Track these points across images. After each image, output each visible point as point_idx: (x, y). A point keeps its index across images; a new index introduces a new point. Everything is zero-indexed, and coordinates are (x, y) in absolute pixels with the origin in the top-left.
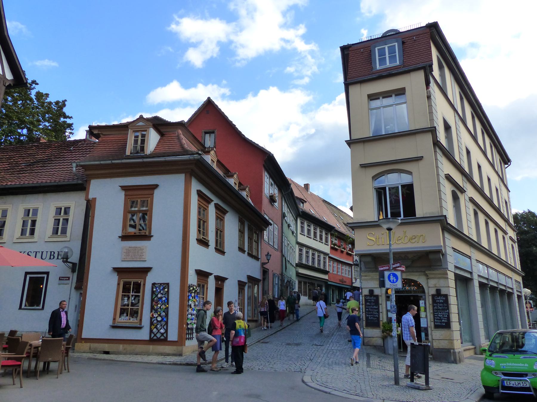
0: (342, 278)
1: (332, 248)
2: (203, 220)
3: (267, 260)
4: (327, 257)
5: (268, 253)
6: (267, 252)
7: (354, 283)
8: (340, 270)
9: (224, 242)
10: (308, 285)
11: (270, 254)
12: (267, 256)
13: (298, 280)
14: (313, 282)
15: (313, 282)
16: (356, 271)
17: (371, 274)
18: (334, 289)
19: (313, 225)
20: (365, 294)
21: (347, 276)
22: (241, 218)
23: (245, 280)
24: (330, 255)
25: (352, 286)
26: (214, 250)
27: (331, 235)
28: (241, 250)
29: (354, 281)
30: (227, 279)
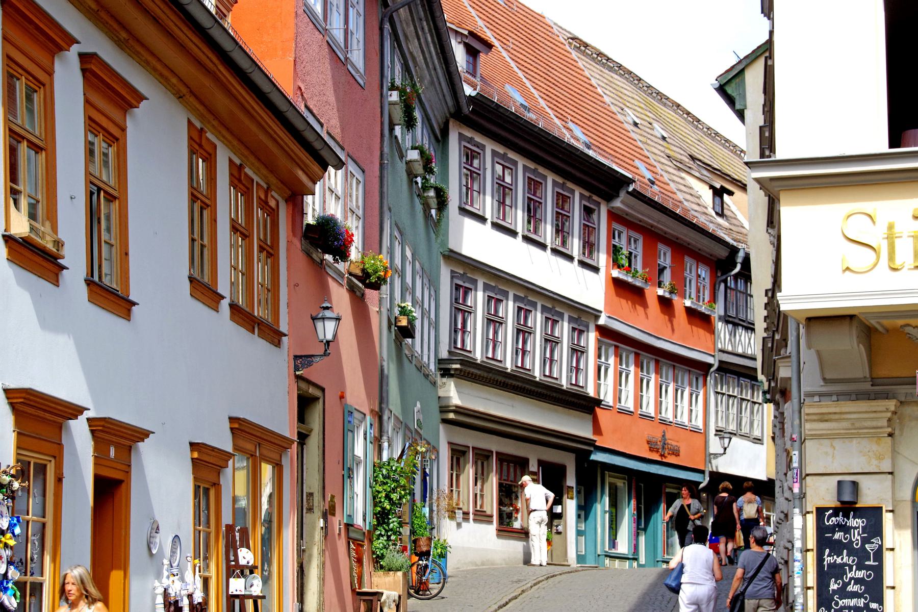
2: (28, 141)
7: (716, 456)
8: (650, 395)
13: (449, 443)
18: (620, 483)
22: (201, 131)
26: (83, 289)
27: (614, 216)
29: (715, 445)
30: (143, 435)
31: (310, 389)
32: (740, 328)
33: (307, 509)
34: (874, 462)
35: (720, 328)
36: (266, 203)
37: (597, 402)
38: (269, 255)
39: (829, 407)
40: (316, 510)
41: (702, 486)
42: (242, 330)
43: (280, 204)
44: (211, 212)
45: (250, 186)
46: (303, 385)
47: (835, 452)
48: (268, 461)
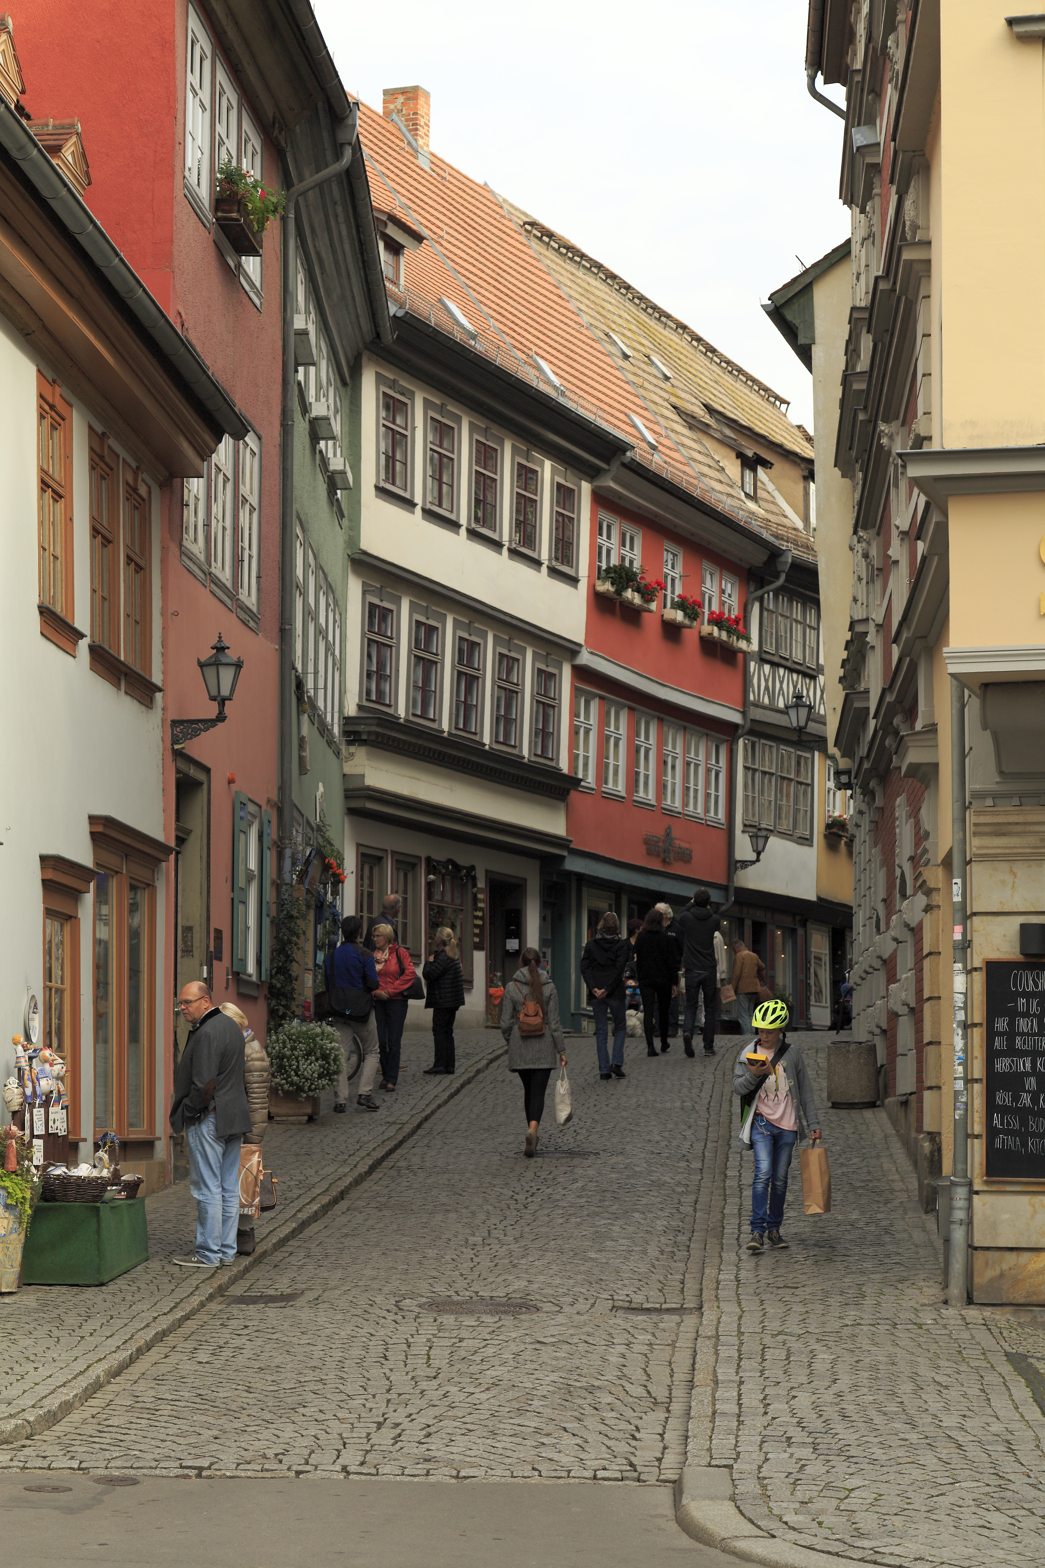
0: (661, 833)
3: (213, 699)
5: (220, 649)
6: (214, 641)
7: (745, 864)
8: (649, 769)
10: (430, 885)
11: (232, 655)
12: (210, 672)
13: (358, 845)
14: (464, 856)
15: (464, 856)
16: (758, 775)
19: (472, 426)
20: (995, 955)
21: (700, 810)
27: (600, 499)
29: (743, 848)
31: (192, 771)
32: (781, 671)
33: (183, 951)
35: (752, 670)
36: (135, 490)
37: (574, 782)
38: (139, 568)
39: (1009, 815)
40: (196, 953)
41: (723, 908)
42: (107, 684)
43: (153, 490)
44: (65, 505)
45: (113, 465)
46: (183, 766)
47: (1016, 880)
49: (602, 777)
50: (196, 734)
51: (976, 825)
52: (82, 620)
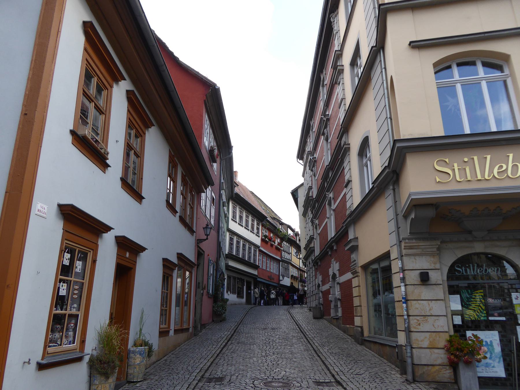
1: (262, 240)
3: (205, 235)
4: (258, 250)
7: (281, 280)
9: (142, 179)
10: (238, 281)
12: (205, 229)
14: (243, 277)
15: (243, 277)
17: (422, 243)
19: (245, 212)
23: (174, 260)
24: (261, 248)
25: (279, 284)
27: (262, 226)
28: (171, 207)
29: (281, 278)
33: (198, 287)
34: (433, 265)
39: (414, 243)
48: (188, 271)
49: (262, 267)
50: (202, 242)
51: (405, 246)
52: (178, 208)
